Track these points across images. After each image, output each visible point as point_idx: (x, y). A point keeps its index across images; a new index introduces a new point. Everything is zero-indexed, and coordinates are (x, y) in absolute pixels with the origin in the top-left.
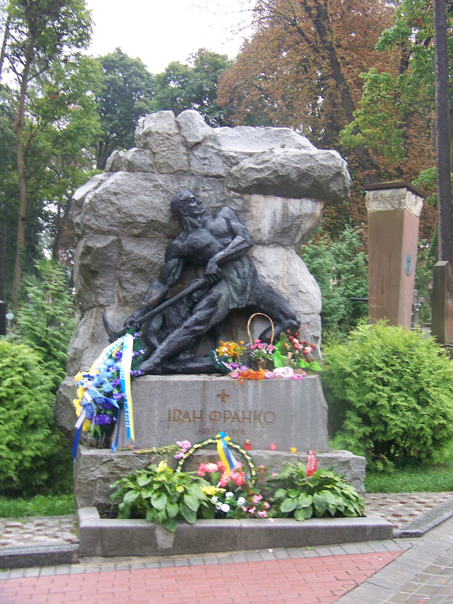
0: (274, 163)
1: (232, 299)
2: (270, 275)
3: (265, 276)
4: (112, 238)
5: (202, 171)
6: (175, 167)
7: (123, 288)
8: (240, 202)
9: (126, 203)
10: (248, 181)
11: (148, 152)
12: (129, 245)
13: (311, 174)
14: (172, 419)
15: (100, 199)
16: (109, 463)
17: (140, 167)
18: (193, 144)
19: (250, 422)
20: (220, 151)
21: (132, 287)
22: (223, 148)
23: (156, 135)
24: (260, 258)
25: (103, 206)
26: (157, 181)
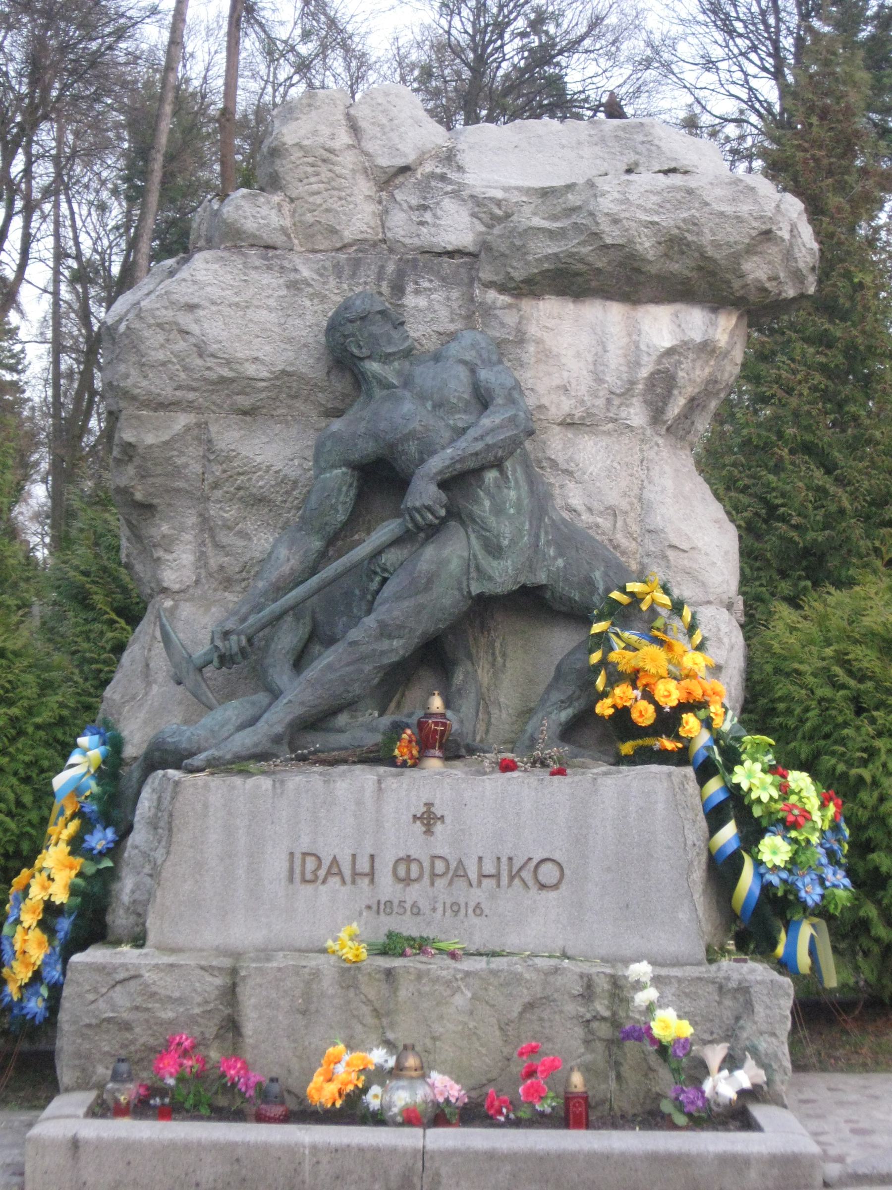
1: (478, 568)
2: (596, 505)
3: (580, 508)
4: (182, 420)
5: (416, 241)
6: (346, 233)
7: (218, 546)
8: (510, 319)
9: (214, 329)
10: (527, 263)
11: (276, 198)
12: (229, 436)
13: (690, 237)
15: (152, 321)
16: (132, 983)
17: (255, 236)
18: (393, 170)
19: (499, 886)
20: (461, 186)
21: (241, 543)
23: (297, 154)
24: (567, 462)
25: (161, 338)
26: (296, 270)
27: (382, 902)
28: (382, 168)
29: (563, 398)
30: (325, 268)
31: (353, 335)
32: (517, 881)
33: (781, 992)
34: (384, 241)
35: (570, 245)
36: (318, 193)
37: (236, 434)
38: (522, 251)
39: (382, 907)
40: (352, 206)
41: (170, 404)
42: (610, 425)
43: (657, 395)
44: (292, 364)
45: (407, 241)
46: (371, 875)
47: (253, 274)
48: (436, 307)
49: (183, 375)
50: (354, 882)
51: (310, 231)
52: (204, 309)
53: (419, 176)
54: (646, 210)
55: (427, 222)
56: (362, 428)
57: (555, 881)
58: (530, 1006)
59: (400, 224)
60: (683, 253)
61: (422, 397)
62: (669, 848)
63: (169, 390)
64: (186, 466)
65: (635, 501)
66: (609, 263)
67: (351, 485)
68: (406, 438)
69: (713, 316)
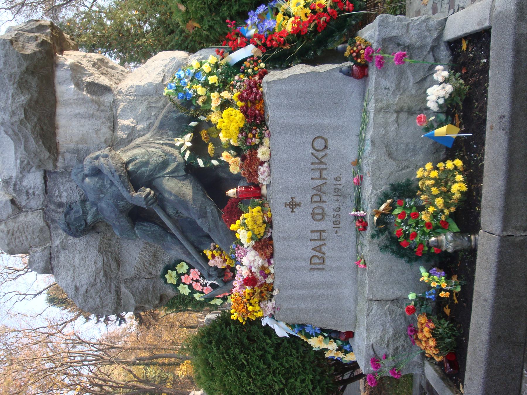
0: (12, 124)
3: (148, 122)
4: (123, 289)
5: (42, 196)
8: (68, 156)
10: (41, 151)
13: (18, 78)
14: (321, 266)
15: (84, 304)
17: (47, 262)
18: (13, 206)
19: (326, 169)
20: (17, 177)
22: (14, 175)
25: (90, 300)
26: (57, 246)
27: (334, 226)
28: (13, 211)
29: (102, 131)
30: (56, 234)
31: (76, 228)
32: (323, 160)
33: (385, 21)
34: (43, 209)
35: (29, 133)
36: (26, 237)
37: (128, 267)
38: (36, 154)
39: (336, 226)
40: (30, 223)
41: (118, 295)
42: (114, 109)
43: (98, 89)
44: (96, 248)
45: (42, 200)
46: (320, 232)
47: (61, 263)
48: (66, 188)
49: (105, 290)
50: (324, 240)
51: (42, 239)
52: (76, 284)
53: (15, 195)
54: (7, 99)
55: (33, 192)
56: (116, 223)
57: (323, 141)
58: (390, 155)
59: (36, 203)
60: (26, 81)
61: (100, 199)
62: (305, 82)
63: (111, 295)
64: (143, 286)
65: (144, 98)
66: (34, 115)
67: (143, 225)
68: (117, 206)
69: (60, 66)
